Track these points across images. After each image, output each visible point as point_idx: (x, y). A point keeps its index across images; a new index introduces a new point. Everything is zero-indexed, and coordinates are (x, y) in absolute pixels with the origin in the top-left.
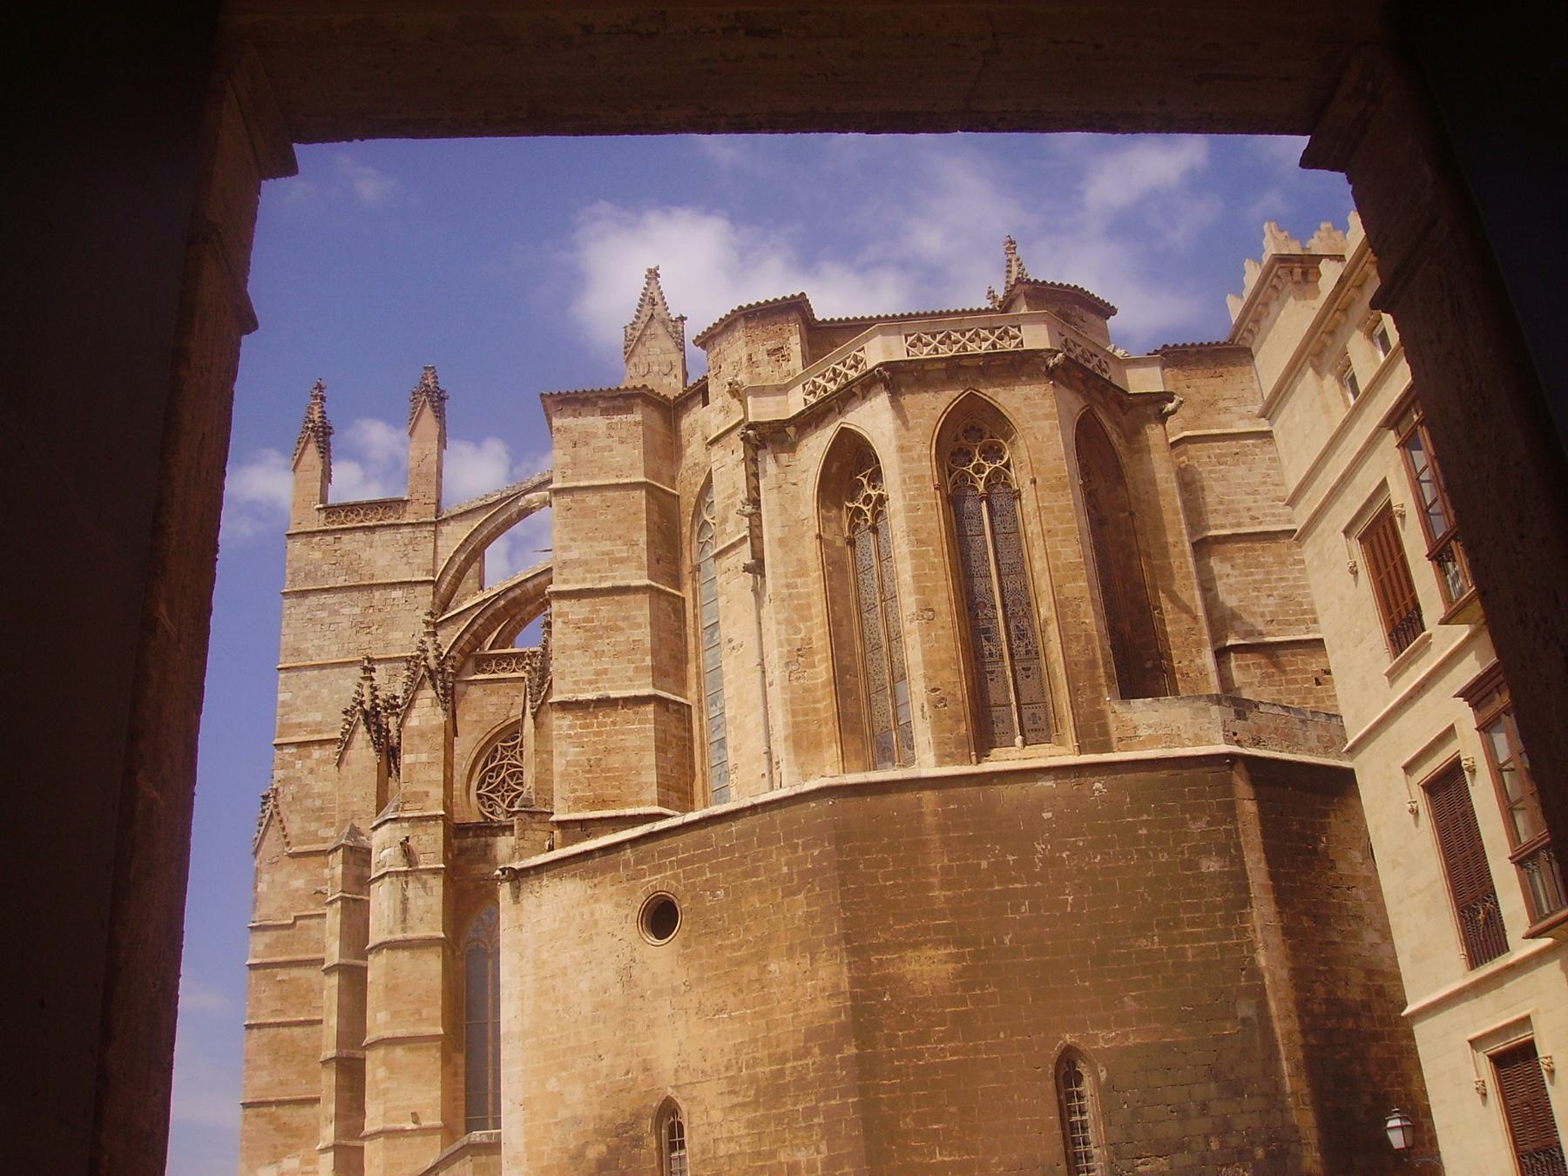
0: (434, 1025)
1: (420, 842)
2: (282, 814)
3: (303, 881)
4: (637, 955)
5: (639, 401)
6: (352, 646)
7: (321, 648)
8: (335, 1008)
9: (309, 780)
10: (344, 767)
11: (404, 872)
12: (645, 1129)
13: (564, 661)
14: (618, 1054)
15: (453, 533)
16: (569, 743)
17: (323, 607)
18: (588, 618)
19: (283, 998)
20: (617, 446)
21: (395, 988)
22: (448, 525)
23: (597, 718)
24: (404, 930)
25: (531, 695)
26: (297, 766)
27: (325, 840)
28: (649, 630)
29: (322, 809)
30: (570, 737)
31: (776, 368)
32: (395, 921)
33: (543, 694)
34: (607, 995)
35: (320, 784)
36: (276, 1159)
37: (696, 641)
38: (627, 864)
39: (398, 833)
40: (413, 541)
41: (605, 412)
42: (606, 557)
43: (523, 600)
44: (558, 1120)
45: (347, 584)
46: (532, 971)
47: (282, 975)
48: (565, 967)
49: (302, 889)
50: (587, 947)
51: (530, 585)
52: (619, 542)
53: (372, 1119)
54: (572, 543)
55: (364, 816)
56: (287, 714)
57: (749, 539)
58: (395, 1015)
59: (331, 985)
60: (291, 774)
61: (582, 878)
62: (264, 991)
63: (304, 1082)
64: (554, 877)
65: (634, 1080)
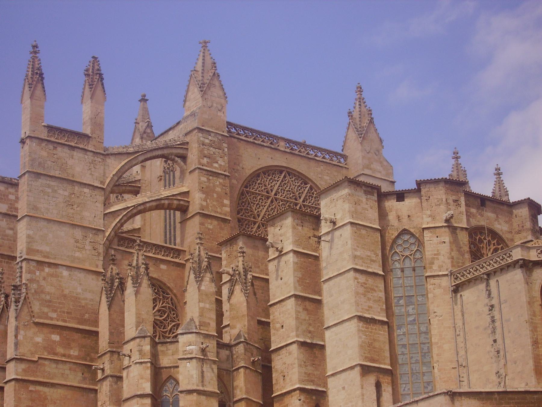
6: (64, 213)
9: (43, 283)
10: (139, 296)
11: (203, 359)
13: (358, 299)
15: (111, 163)
17: (49, 186)
19: (32, 400)
20: (369, 208)
22: (109, 158)
23: (370, 326)
24: (203, 386)
27: (52, 319)
31: (456, 209)
38: (496, 399)
39: (198, 339)
40: (93, 162)
41: (366, 193)
45: (60, 176)
47: (32, 388)
49: (40, 343)
52: (372, 253)
61: (478, 400)
62: (23, 394)
64: (467, 397)
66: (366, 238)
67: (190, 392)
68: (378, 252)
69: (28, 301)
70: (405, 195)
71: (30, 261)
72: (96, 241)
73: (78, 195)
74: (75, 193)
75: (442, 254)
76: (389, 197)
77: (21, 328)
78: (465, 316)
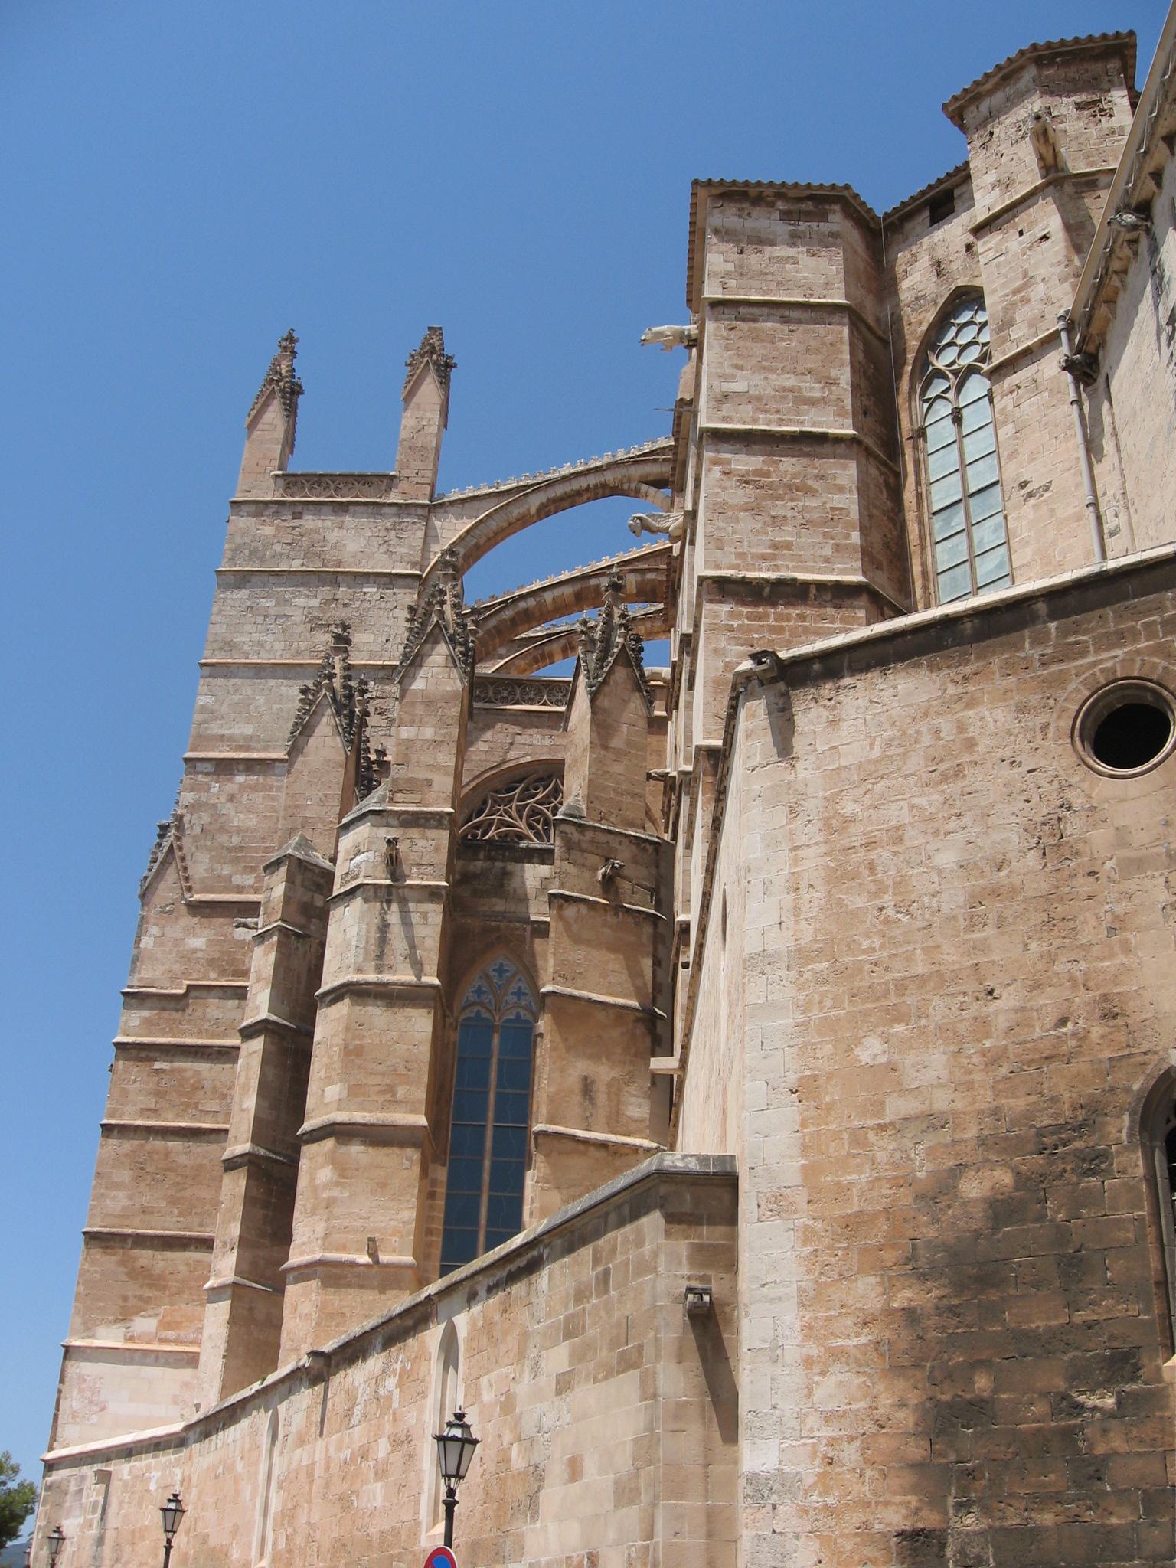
0: (413, 1111)
1: (414, 848)
2: (185, 851)
3: (204, 940)
4: (1077, 799)
5: (837, 207)
7: (261, 644)
8: (254, 1083)
9: (228, 809)
12: (1113, 1136)
13: (722, 525)
14: (1037, 986)
16: (730, 638)
18: (761, 470)
19: (159, 1094)
21: (359, 1051)
24: (379, 969)
25: (588, 671)
26: (212, 790)
27: (240, 889)
28: (856, 496)
29: (241, 848)
30: (731, 629)
31: (1091, 125)
32: (366, 953)
33: (606, 669)
34: (1002, 874)
35: (242, 816)
36: (125, 1315)
37: (920, 530)
41: (786, 216)
42: (790, 395)
43: (537, 614)
44: (887, 1120)
46: (819, 838)
48: (899, 827)
50: (953, 788)
51: (548, 596)
53: (304, 1244)
54: (739, 372)
55: (320, 825)
56: (206, 721)
57: (1063, 334)
58: (355, 1091)
59: (250, 1051)
60: (203, 799)
62: (135, 1081)
63: (176, 1211)
65: (1081, 1037)
66: (782, 339)
67: (338, 994)
68: (834, 373)
69: (178, 854)
70: (956, 193)
71: (198, 764)
72: (384, 695)
73: (346, 601)
74: (337, 597)
75: (1039, 279)
76: (908, 226)
77: (152, 920)
78: (1122, 437)
